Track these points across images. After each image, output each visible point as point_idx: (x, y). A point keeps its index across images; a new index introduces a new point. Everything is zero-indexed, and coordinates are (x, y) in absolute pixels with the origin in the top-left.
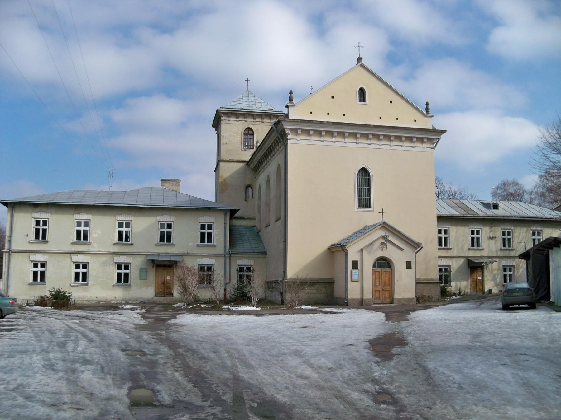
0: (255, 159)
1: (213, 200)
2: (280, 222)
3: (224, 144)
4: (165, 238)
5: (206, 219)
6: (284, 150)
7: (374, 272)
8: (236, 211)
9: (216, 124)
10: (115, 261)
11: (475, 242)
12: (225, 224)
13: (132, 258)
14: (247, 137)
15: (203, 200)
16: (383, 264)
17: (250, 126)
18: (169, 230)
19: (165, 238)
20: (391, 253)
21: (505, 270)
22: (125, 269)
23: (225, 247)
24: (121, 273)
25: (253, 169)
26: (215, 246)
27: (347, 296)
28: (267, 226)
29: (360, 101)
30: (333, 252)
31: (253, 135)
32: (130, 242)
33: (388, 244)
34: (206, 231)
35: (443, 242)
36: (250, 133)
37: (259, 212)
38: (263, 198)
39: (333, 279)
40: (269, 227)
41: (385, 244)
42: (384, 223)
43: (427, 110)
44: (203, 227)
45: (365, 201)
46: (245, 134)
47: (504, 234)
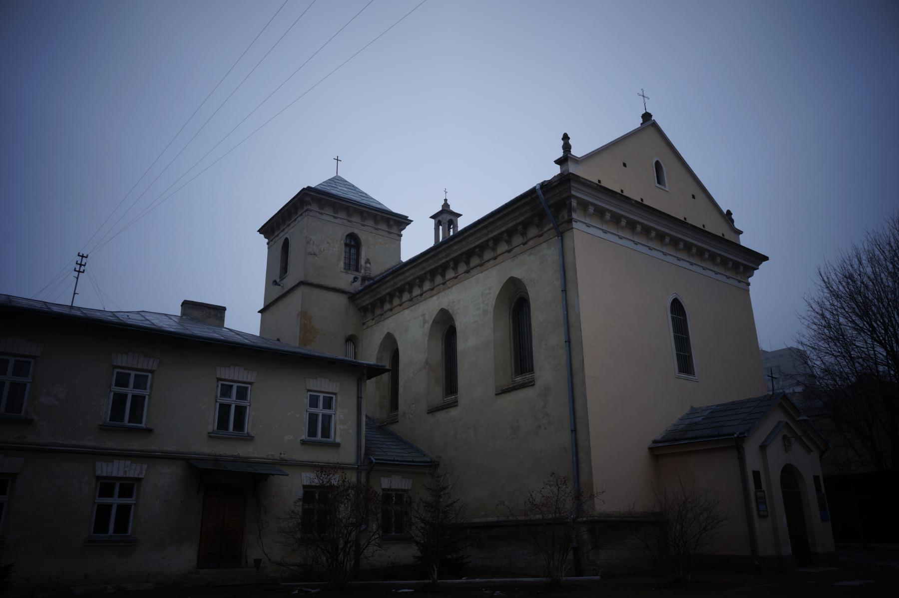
0: (392, 283)
3: (310, 254)
4: (231, 420)
5: (323, 384)
9: (268, 230)
10: (98, 473)
13: (145, 467)
17: (356, 231)
18: (242, 403)
22: (121, 495)
23: (359, 447)
24: (110, 507)
26: (337, 445)
32: (143, 425)
34: (320, 411)
40: (454, 412)
44: (314, 402)
46: (346, 245)
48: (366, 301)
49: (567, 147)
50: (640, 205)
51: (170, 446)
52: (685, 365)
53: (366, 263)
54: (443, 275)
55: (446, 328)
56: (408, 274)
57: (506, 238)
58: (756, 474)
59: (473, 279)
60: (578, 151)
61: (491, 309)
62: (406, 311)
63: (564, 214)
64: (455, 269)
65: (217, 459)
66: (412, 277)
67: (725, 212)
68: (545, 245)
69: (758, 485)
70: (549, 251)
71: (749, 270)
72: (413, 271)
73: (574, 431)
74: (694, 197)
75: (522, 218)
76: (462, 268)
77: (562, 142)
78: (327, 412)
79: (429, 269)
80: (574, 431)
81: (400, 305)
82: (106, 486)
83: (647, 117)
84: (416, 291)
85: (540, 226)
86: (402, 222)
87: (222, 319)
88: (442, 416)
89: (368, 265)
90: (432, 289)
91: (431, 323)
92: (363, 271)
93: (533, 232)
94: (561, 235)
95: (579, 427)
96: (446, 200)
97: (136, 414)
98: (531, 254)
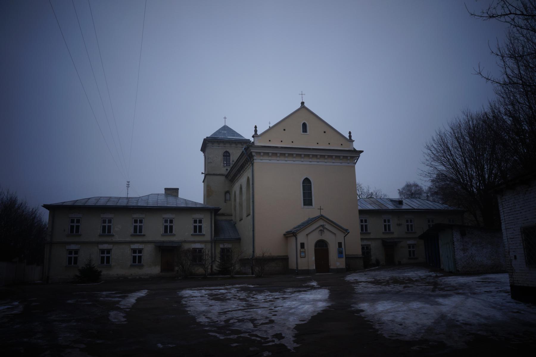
1: (202, 202)
2: (250, 217)
4: (168, 230)
5: (198, 216)
6: (251, 167)
8: (219, 209)
9: (203, 149)
11: (387, 228)
12: (211, 219)
15: (195, 202)
17: (228, 150)
18: (171, 224)
19: (168, 230)
20: (327, 237)
21: (409, 247)
22: (139, 253)
23: (211, 235)
25: (230, 180)
26: (204, 235)
27: (297, 268)
28: (241, 220)
29: (303, 132)
30: (287, 237)
31: (229, 156)
33: (325, 230)
34: (198, 224)
35: (364, 229)
37: (235, 210)
38: (238, 200)
39: (287, 256)
40: (242, 221)
41: (323, 231)
42: (322, 216)
43: (350, 136)
44: (195, 222)
45: (308, 201)
46: (224, 156)
47: (407, 221)
49: (256, 131)
51: (150, 239)
60: (259, 133)
65: (163, 242)
74: (325, 132)
77: (254, 129)
78: (200, 224)
82: (134, 251)
83: (303, 103)
87: (178, 193)
94: (253, 164)
97: (141, 231)
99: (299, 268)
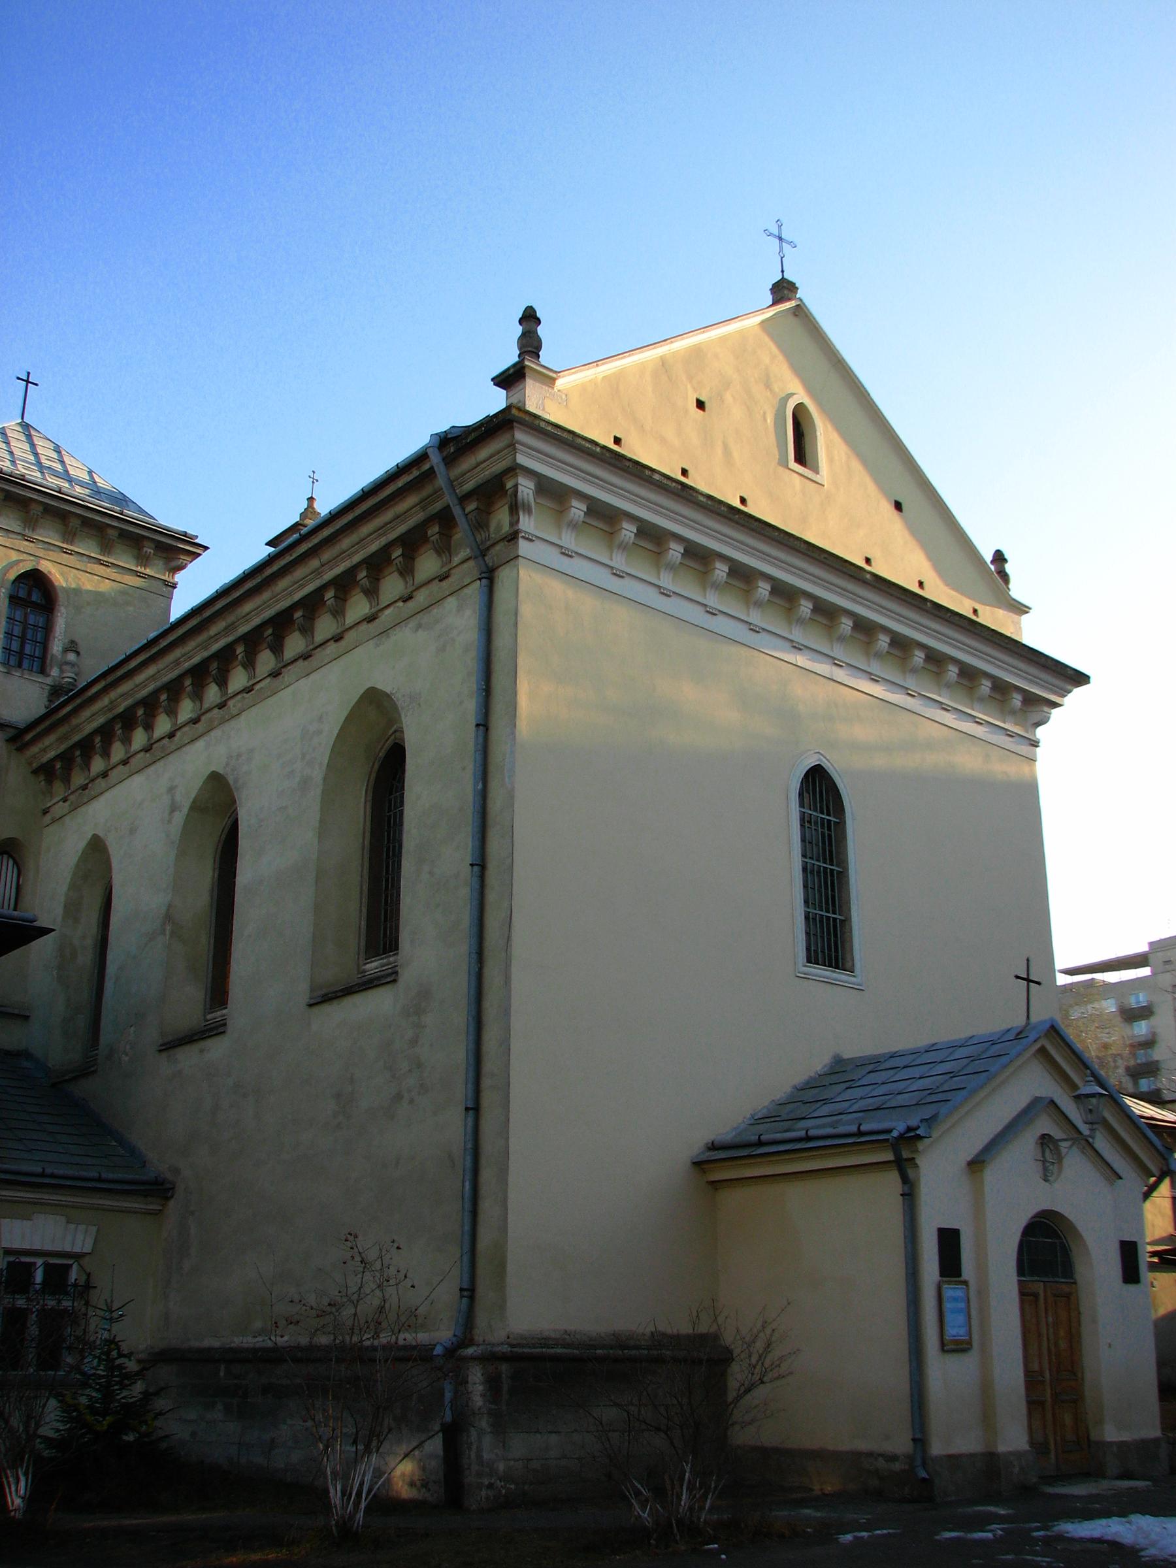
0: (105, 701)
6: (475, 591)
7: (1025, 1295)
14: (19, 615)
16: (1047, 1248)
17: (46, 567)
27: (920, 1441)
36: (34, 598)
40: (216, 1049)
46: (14, 600)
48: (49, 748)
49: (530, 344)
50: (737, 518)
52: (828, 942)
53: (66, 650)
54: (222, 683)
55: (218, 824)
56: (140, 678)
57: (365, 582)
58: (949, 1240)
59: (286, 694)
61: (317, 774)
62: (138, 780)
63: (501, 518)
64: (250, 664)
66: (151, 688)
67: (988, 557)
68: (452, 602)
69: (950, 1264)
70: (459, 618)
71: (1036, 708)
72: (151, 670)
73: (474, 1109)
75: (402, 529)
76: (266, 660)
79: (187, 665)
80: (474, 1109)
81: (125, 762)
84: (163, 725)
85: (445, 548)
86: (176, 549)
88: (188, 1058)
89: (71, 657)
90: (195, 721)
91: (186, 810)
92: (55, 672)
93: (428, 564)
94: (489, 576)
95: (489, 1099)
96: (311, 499)
98: (419, 626)
99: (937, 1448)
